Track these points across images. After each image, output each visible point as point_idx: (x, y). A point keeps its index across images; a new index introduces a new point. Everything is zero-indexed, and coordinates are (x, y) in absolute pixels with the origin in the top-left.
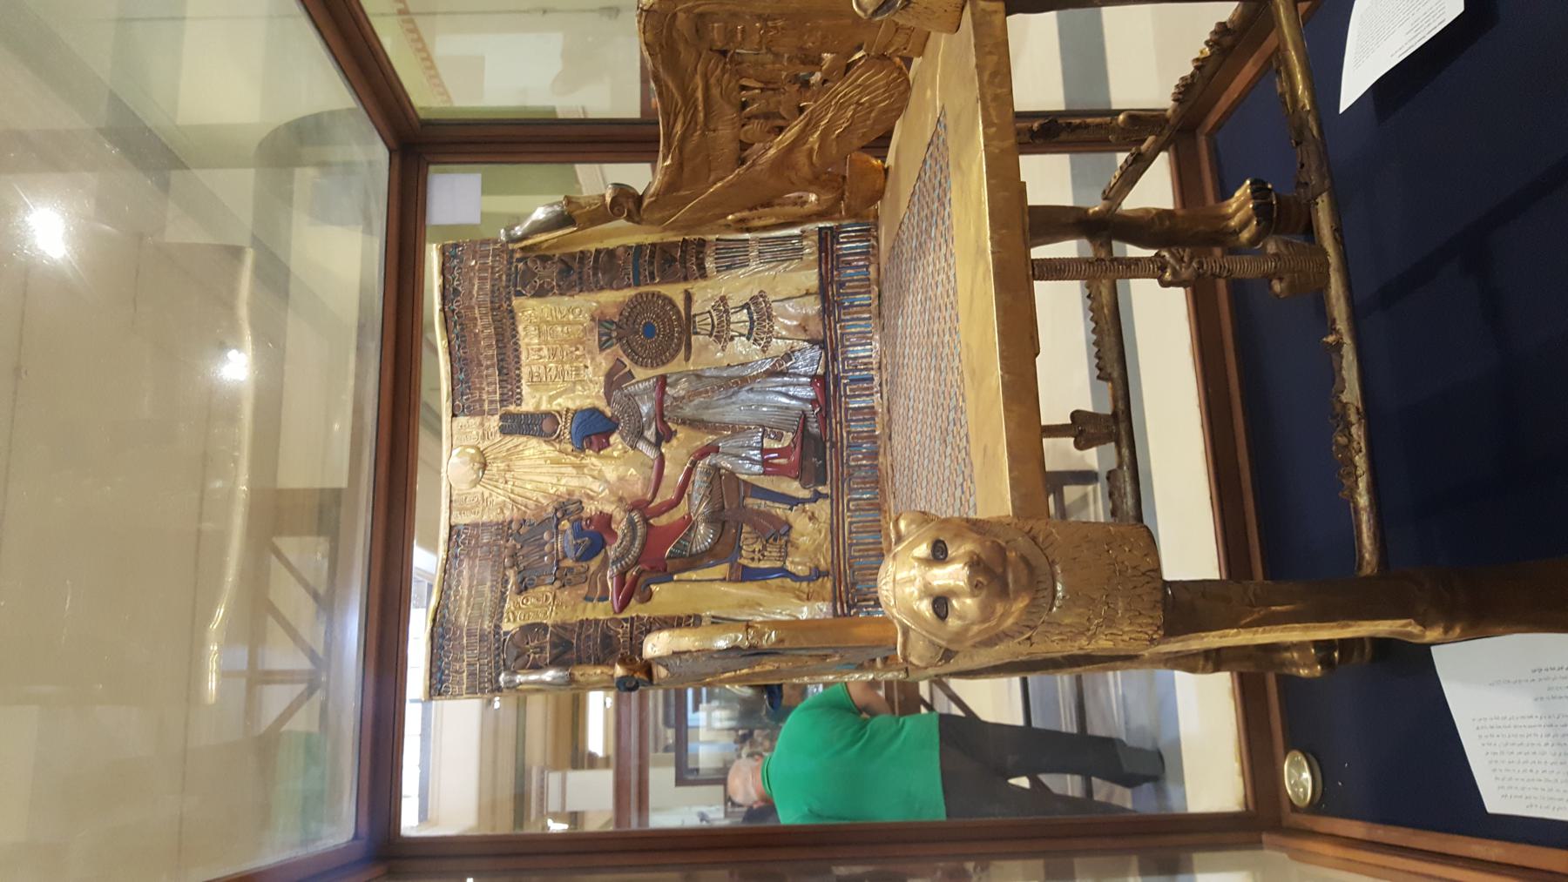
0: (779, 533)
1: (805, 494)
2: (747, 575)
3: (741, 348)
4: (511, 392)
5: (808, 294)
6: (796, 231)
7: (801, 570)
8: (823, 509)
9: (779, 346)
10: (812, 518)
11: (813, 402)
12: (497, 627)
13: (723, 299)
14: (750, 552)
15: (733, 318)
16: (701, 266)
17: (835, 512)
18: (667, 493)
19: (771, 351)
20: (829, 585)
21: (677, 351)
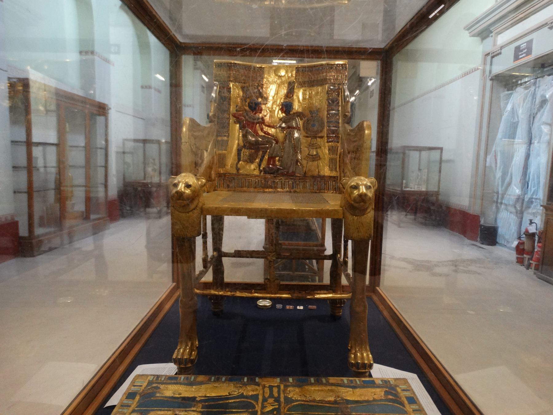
0: (251, 160)
1: (261, 169)
2: (239, 151)
3: (305, 150)
4: (302, 85)
5: (319, 172)
6: (338, 169)
7: (239, 166)
8: (256, 172)
9: (304, 162)
10: (254, 169)
11: (288, 172)
12: (232, 81)
13: (320, 147)
14: (246, 152)
15: (314, 150)
16: (330, 142)
17: (256, 176)
18: (266, 129)
19: (303, 160)
20: (234, 172)
21: (306, 133)
